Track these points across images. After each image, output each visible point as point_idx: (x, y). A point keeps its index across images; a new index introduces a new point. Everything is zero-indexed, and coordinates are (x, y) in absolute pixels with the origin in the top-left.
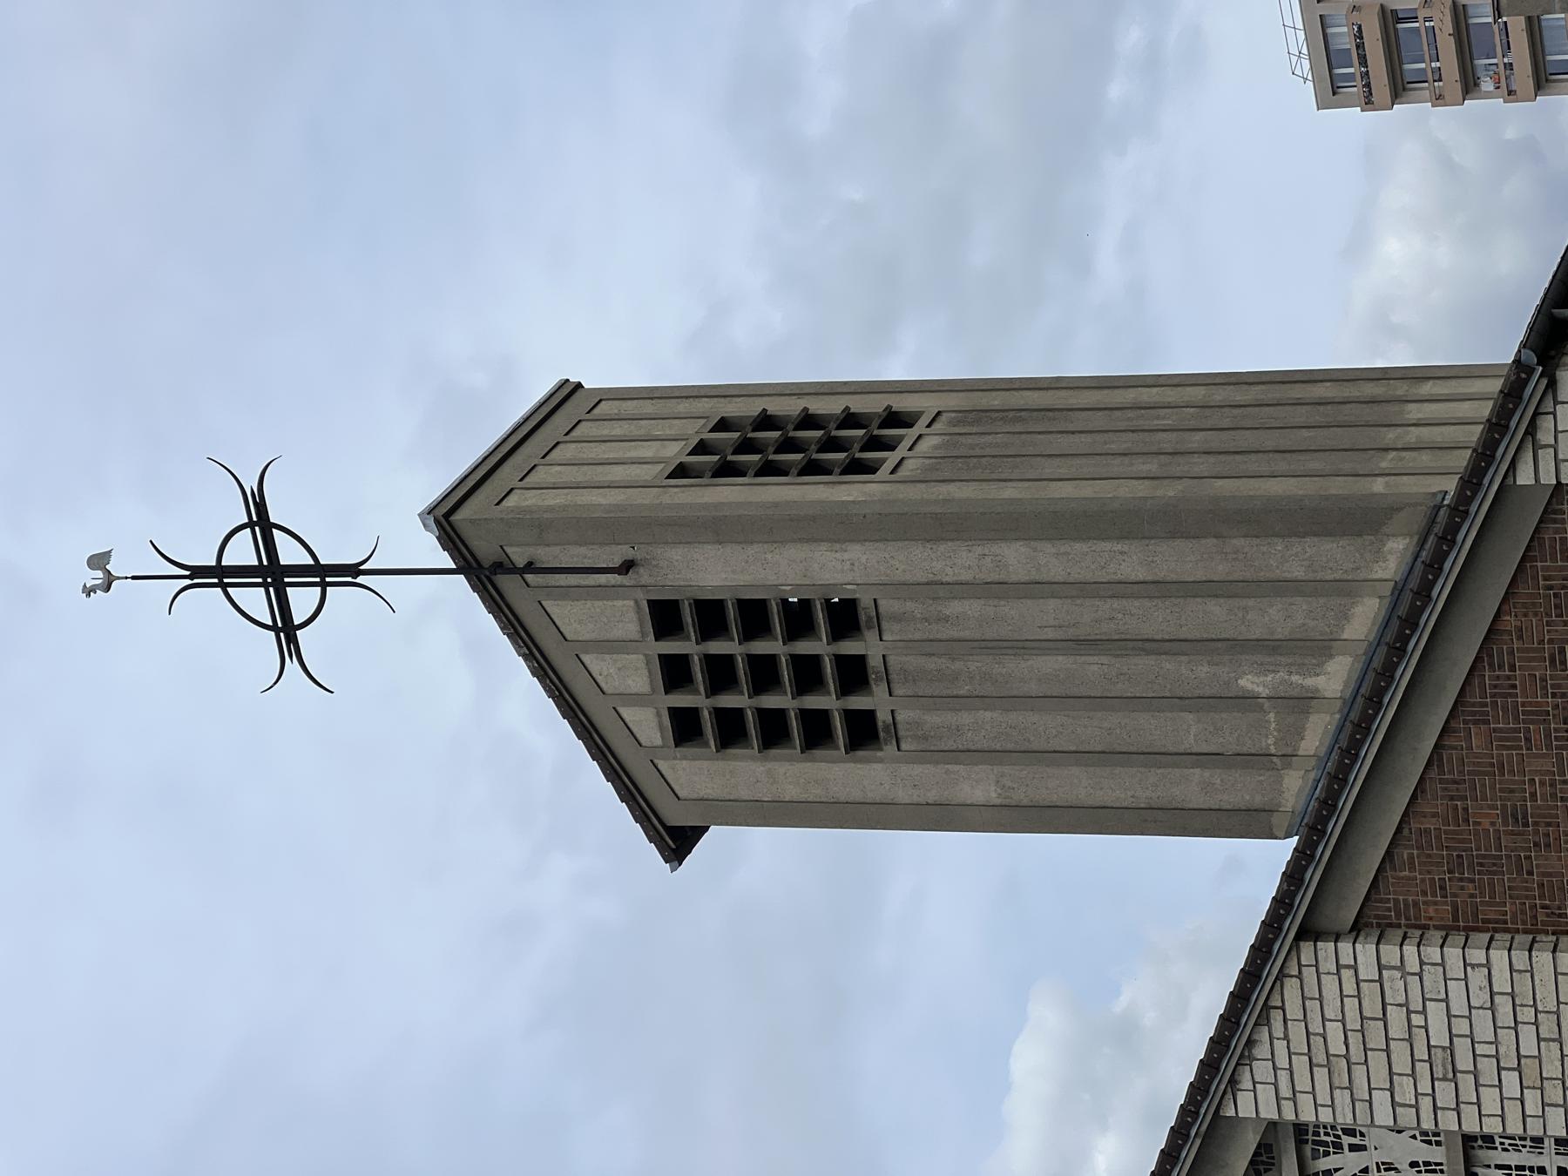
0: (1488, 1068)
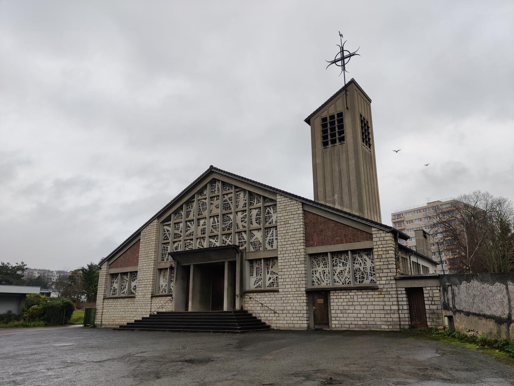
0: (286, 228)
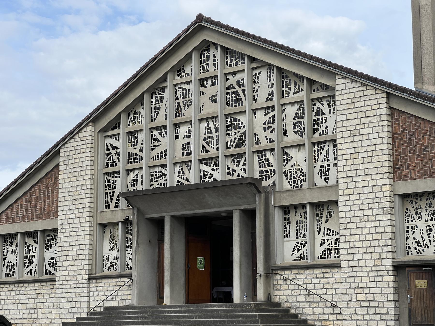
0: (355, 145)
